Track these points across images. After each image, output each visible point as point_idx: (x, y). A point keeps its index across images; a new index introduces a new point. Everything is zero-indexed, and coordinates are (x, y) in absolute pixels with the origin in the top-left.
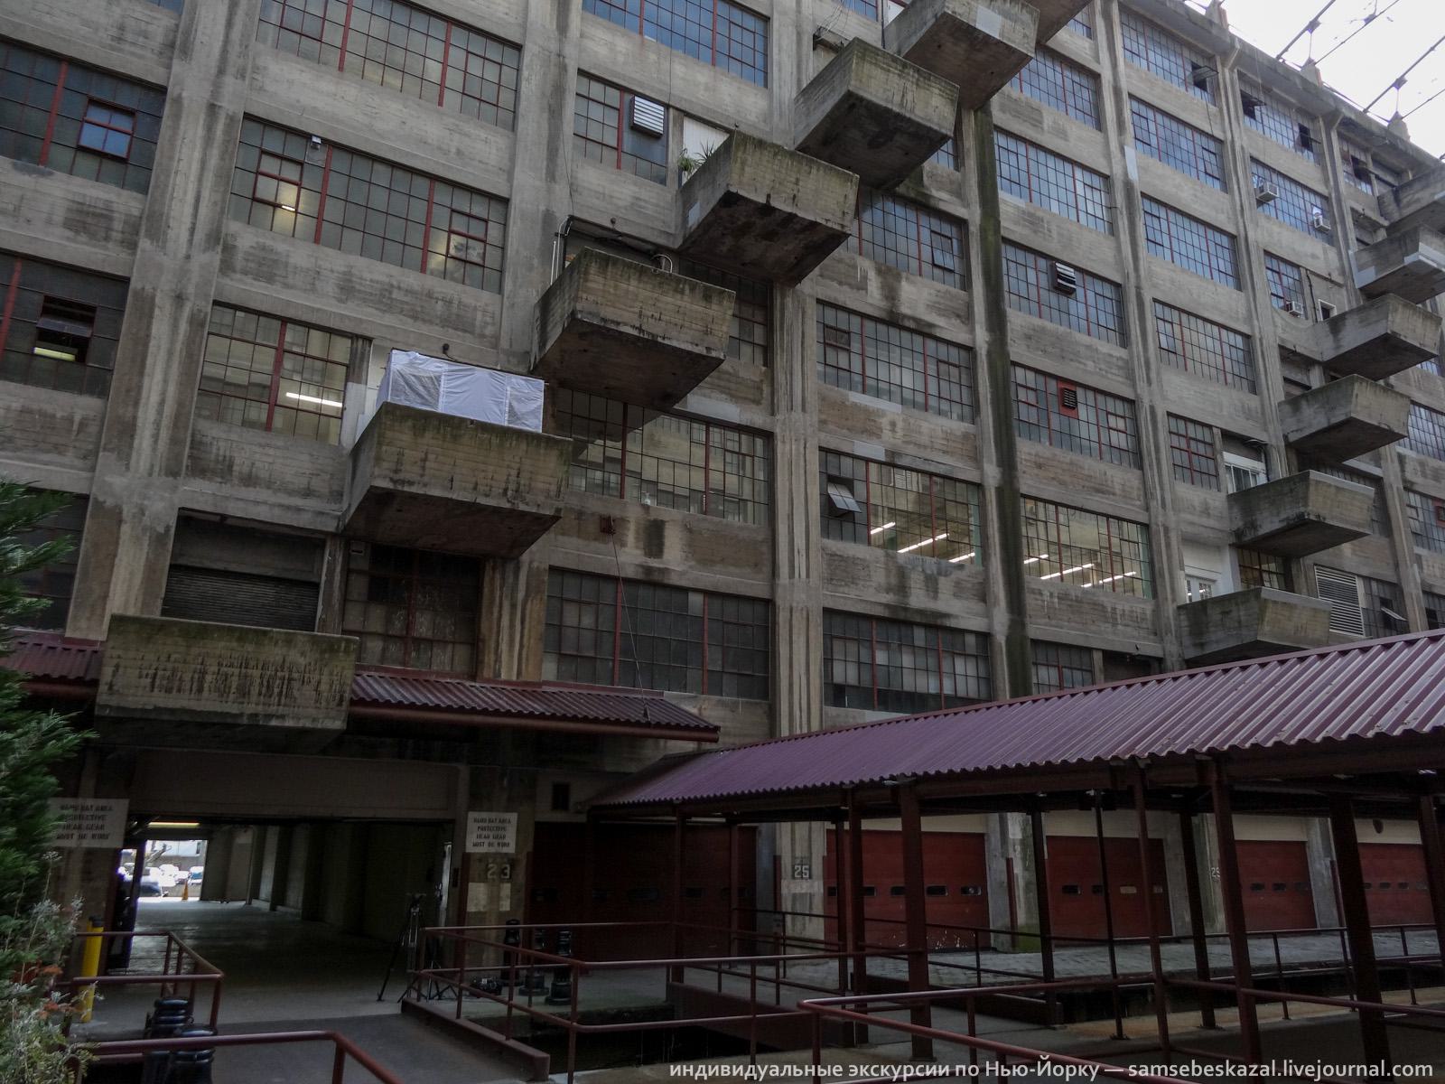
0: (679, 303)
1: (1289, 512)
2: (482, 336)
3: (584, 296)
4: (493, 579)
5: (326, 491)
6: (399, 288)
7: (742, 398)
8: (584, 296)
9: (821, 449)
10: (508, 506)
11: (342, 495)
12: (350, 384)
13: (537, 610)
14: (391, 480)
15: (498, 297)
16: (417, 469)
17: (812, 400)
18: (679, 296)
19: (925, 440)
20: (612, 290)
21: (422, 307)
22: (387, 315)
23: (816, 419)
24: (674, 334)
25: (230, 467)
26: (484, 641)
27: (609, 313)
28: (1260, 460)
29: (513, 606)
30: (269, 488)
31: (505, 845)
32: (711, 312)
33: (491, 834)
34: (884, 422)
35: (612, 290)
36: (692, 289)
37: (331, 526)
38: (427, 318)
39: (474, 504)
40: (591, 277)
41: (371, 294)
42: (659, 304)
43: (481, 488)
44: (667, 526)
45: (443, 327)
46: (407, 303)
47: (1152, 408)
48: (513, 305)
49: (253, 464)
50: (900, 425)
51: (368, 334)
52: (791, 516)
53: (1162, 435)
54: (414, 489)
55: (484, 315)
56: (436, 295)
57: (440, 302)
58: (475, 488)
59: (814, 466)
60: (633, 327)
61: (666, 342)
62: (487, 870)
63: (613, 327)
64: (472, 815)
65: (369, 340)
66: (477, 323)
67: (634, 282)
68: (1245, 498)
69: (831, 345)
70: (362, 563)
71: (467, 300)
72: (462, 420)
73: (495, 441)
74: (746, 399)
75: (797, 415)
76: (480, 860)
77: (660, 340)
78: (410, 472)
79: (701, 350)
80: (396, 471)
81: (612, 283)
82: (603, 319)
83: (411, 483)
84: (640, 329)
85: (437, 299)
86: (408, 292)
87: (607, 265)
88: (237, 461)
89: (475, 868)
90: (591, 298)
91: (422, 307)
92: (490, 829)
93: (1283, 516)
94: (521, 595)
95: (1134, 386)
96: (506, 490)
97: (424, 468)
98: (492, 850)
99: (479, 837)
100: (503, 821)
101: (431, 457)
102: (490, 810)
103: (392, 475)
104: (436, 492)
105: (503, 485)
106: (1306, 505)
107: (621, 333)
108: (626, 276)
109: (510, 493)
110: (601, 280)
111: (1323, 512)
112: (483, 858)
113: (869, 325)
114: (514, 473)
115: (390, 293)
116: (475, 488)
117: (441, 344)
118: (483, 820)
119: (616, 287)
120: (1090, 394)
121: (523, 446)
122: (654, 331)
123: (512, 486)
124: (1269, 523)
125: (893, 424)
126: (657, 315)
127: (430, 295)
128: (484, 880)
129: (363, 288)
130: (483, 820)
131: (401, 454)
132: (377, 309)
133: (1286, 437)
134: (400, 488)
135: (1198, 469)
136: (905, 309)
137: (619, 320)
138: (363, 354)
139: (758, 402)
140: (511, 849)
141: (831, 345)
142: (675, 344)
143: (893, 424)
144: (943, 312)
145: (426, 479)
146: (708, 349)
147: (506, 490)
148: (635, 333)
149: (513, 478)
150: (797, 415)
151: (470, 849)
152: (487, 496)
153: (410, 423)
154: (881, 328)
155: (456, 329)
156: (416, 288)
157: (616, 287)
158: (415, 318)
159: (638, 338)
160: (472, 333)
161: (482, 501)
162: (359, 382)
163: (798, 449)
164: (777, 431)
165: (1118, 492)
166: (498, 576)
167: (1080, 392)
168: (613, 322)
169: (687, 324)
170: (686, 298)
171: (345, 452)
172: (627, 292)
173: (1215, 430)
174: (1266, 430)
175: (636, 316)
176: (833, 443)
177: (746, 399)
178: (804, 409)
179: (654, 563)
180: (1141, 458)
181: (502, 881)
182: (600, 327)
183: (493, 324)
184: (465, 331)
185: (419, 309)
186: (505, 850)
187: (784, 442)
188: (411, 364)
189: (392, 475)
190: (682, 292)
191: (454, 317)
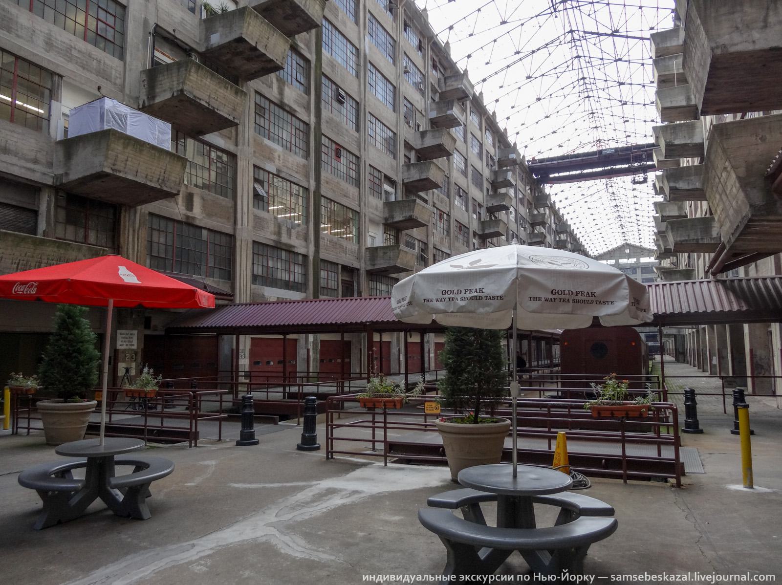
0: (226, 94)
1: (407, 214)
2: (115, 84)
3: (188, 83)
7: (223, 135)
8: (188, 83)
9: (255, 166)
10: (159, 187)
12: (53, 101)
13: (144, 234)
14: (111, 168)
15: (122, 63)
16: (123, 165)
17: (251, 141)
18: (225, 90)
19: (290, 166)
20: (199, 82)
21: (86, 62)
22: (70, 64)
23: (252, 151)
26: (122, 247)
27: (197, 93)
28: (393, 188)
29: (134, 231)
31: (133, 345)
32: (237, 100)
33: (127, 340)
34: (276, 155)
35: (199, 82)
36: (231, 88)
39: (146, 184)
40: (192, 74)
41: (61, 50)
42: (217, 93)
43: (149, 177)
45: (97, 75)
46: (79, 58)
47: (365, 161)
48: (130, 70)
50: (282, 157)
51: (61, 73)
53: (367, 173)
54: (121, 175)
55: (116, 73)
56: (93, 56)
57: (95, 61)
58: (146, 177)
59: (251, 174)
60: (206, 102)
61: (218, 112)
62: (126, 356)
63: (198, 101)
64: (119, 331)
65: (61, 76)
66: (113, 76)
67: (209, 80)
68: (389, 205)
69: (258, 114)
71: (108, 62)
72: (144, 142)
73: (157, 155)
74: (226, 136)
75: (246, 147)
76: (123, 352)
77: (216, 110)
78: (120, 166)
79: (231, 118)
80: (114, 165)
81: (199, 78)
82: (195, 96)
83: (120, 172)
84: (208, 103)
85: (93, 58)
86: (80, 52)
87: (199, 69)
89: (121, 356)
90: (191, 84)
91: (86, 62)
92: (126, 338)
93: (404, 215)
94: (137, 225)
95: (360, 151)
96: (159, 179)
97: (126, 164)
98: (127, 348)
99: (122, 341)
100: (132, 334)
101: (130, 159)
102: (126, 329)
103: (112, 166)
104: (130, 177)
105: (158, 177)
106: (413, 212)
107: (200, 104)
108: (206, 76)
109: (160, 181)
110: (195, 76)
111: (418, 216)
112: (124, 351)
113: (272, 106)
114: (163, 171)
115: (71, 50)
116: (146, 177)
117: (97, 87)
118: (123, 334)
119: (201, 81)
120: (345, 152)
121: (168, 159)
122: (214, 105)
123: (161, 178)
124: (398, 217)
125: (279, 157)
126: (216, 98)
127: (90, 56)
128: (124, 361)
130: (123, 334)
131: (117, 156)
132: (65, 59)
133: (403, 180)
134: (115, 173)
135: (376, 190)
136: (286, 101)
137: (201, 98)
138: (58, 84)
139: (230, 138)
140: (135, 347)
141: (258, 114)
142: (221, 113)
143: (279, 157)
144: (299, 105)
145: (126, 170)
146: (234, 118)
147: (159, 179)
148: (207, 105)
149: (162, 174)
150: (246, 147)
151: (118, 347)
152: (151, 181)
153: (122, 141)
154: (277, 108)
155: (103, 78)
156: (83, 50)
157: (201, 81)
158: (84, 68)
159: (207, 108)
160: (110, 81)
161: (149, 183)
162: (57, 101)
163: (246, 165)
164: (238, 154)
165: (351, 197)
166: (127, 215)
167: (342, 150)
168: (198, 98)
169: (227, 105)
170: (228, 92)
171: (52, 140)
172: (206, 84)
174: (397, 176)
175: (207, 97)
176: (258, 163)
177: (226, 136)
180: (359, 184)
181: (132, 362)
182: (193, 100)
183: (120, 78)
184: (107, 80)
185: (85, 63)
186: (133, 347)
187: (241, 160)
188: (114, 106)
189: (112, 166)
190: (227, 88)
191: (102, 70)
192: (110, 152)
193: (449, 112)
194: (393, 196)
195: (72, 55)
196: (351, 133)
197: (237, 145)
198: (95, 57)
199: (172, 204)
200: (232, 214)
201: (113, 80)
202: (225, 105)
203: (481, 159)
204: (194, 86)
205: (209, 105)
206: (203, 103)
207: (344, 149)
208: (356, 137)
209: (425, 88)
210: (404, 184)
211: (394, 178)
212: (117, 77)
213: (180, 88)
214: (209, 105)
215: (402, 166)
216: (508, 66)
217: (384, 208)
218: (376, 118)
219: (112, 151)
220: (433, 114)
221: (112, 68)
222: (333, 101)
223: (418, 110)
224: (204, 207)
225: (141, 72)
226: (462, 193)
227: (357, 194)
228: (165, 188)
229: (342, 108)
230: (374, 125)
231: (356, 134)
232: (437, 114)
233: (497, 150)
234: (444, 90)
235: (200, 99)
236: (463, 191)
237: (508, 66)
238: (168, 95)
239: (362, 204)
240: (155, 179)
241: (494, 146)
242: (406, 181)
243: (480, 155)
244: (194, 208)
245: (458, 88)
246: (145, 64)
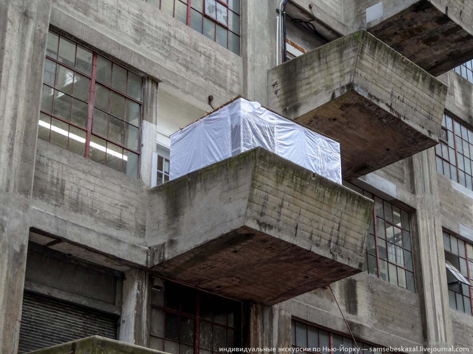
0: (416, 89)
3: (360, 72)
4: (256, 324)
5: (133, 224)
6: (175, 37)
7: (391, 175)
8: (360, 72)
10: (330, 257)
11: (144, 230)
12: (145, 122)
14: (258, 222)
15: (240, 59)
16: (275, 214)
18: (415, 83)
20: (376, 70)
21: (191, 58)
22: (168, 61)
23: (438, 202)
24: (410, 115)
25: (63, 189)
27: (375, 90)
30: (91, 215)
32: (433, 101)
35: (376, 70)
36: (424, 79)
37: (141, 259)
38: (195, 69)
39: (309, 252)
40: (365, 56)
41: (157, 40)
42: (404, 88)
43: (315, 238)
44: (357, 283)
45: (206, 79)
46: (181, 52)
48: (254, 68)
49: (79, 190)
51: (157, 76)
52: (432, 284)
54: (272, 233)
55: (232, 74)
56: (200, 49)
58: (311, 238)
60: (387, 105)
61: (406, 121)
63: (375, 102)
65: (156, 82)
66: (228, 80)
67: (390, 66)
70: (160, 301)
71: (221, 58)
72: (309, 172)
73: (327, 195)
74: (395, 177)
75: (428, 196)
77: (402, 119)
78: (270, 218)
79: (424, 132)
80: (262, 214)
81: (376, 63)
82: (370, 95)
83: (271, 227)
84: (390, 107)
85: (200, 52)
86: (181, 42)
87: (375, 48)
88: (68, 186)
90: (364, 74)
91: (191, 58)
97: (280, 213)
101: (286, 203)
103: (258, 217)
104: (287, 238)
107: (379, 108)
108: (386, 61)
109: (332, 244)
110: (370, 59)
114: (336, 226)
115: (169, 41)
116: (311, 238)
117: (207, 96)
122: (400, 111)
123: (334, 239)
126: (401, 97)
129: (150, 33)
131: (266, 199)
132: (161, 54)
134: (263, 230)
137: (379, 97)
138: (152, 95)
139: (402, 182)
145: (281, 224)
146: (429, 132)
148: (388, 109)
149: (335, 231)
150: (428, 196)
152: (318, 245)
153: (275, 169)
155: (215, 83)
156: (187, 40)
158: (188, 68)
159: (388, 115)
160: (225, 88)
162: (151, 121)
163: (431, 227)
164: (418, 208)
168: (375, 98)
169: (418, 108)
170: (419, 85)
171: (144, 187)
172: (386, 72)
175: (389, 96)
177: (395, 177)
178: (431, 193)
179: (352, 318)
182: (366, 101)
183: (239, 84)
184: (220, 86)
185: (189, 59)
187: (422, 219)
188: (254, 114)
189: (258, 217)
190: (418, 81)
191: (212, 71)
192: (256, 191)
195: (169, 46)
197: (414, 192)
198: (202, 50)
199: (324, 301)
200: (418, 319)
201: (229, 87)
202: (415, 110)
204: (369, 77)
205: (392, 109)
206: (383, 106)
212: (233, 81)
213: (347, 81)
214: (392, 109)
219: (259, 188)
221: (226, 66)
224: (374, 305)
225: (268, 72)
228: (339, 260)
235: (378, 100)
238: (324, 99)
240: (324, 242)
244: (359, 308)
246: (273, 59)
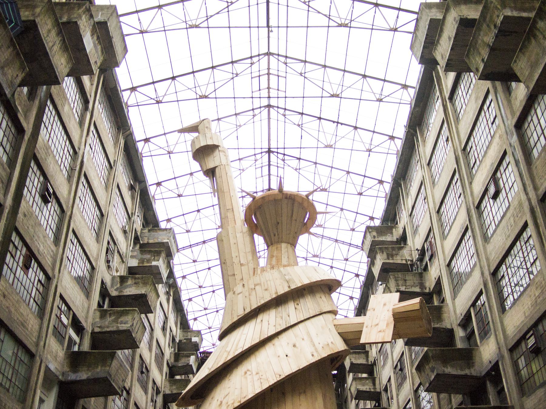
173: (71, 312)
193: (154, 263)
194: (77, 346)
196: (49, 242)
203: (165, 335)
207: (37, 260)
208: (52, 251)
209: (129, 232)
210: (93, 333)
211: (84, 324)
215: (95, 310)
216: (204, 242)
217: (64, 360)
218: (79, 241)
220: (134, 263)
222: (37, 195)
223: (118, 252)
226: (144, 370)
227: (37, 327)
229: (45, 208)
230: (74, 247)
231: (53, 247)
232: (139, 263)
233: (178, 330)
234: (146, 242)
236: (146, 366)
237: (204, 242)
239: (42, 343)
241: (176, 326)
242: (97, 330)
243: (164, 329)
245: (163, 243)
